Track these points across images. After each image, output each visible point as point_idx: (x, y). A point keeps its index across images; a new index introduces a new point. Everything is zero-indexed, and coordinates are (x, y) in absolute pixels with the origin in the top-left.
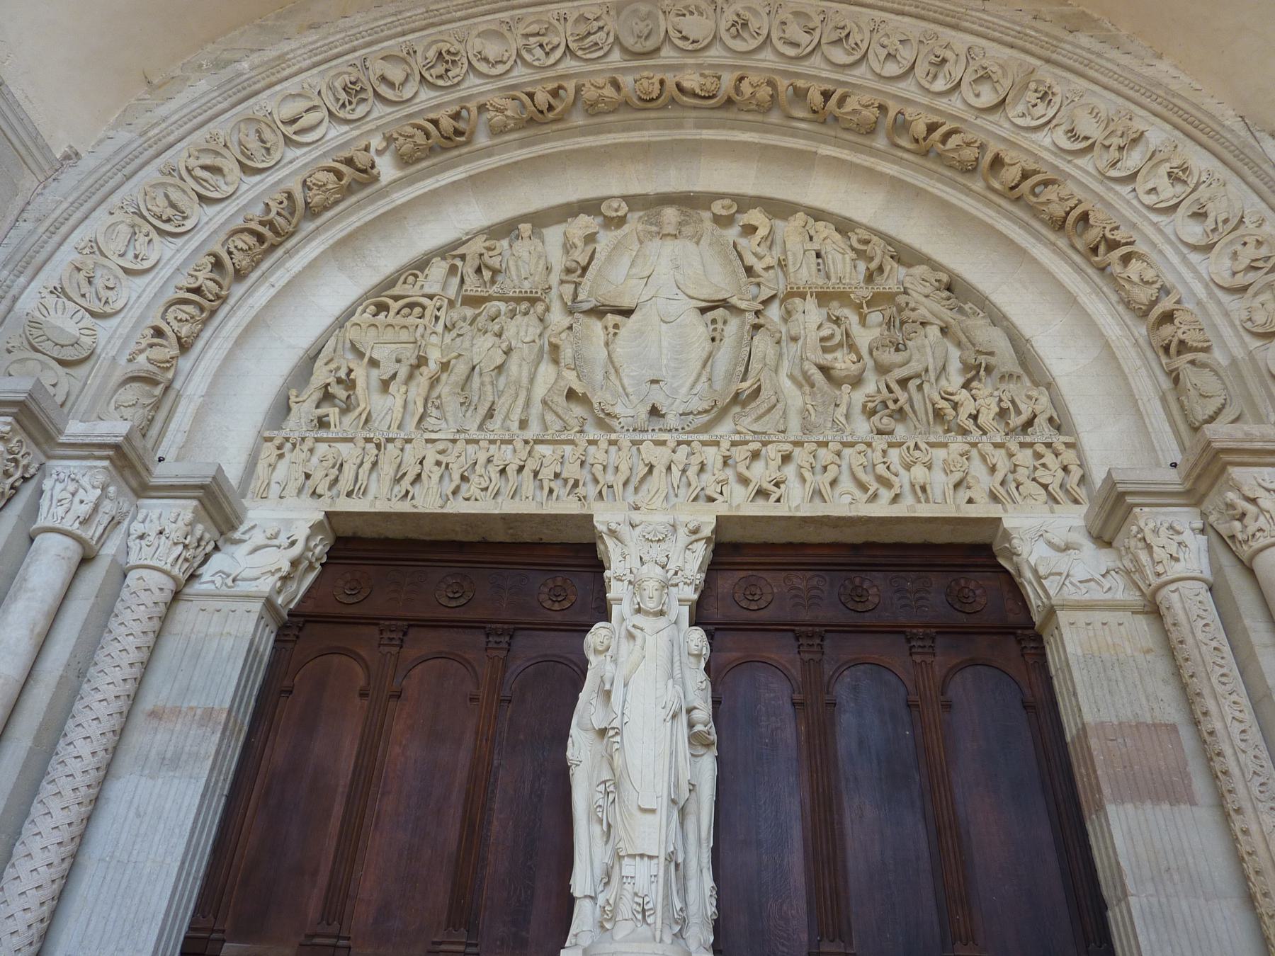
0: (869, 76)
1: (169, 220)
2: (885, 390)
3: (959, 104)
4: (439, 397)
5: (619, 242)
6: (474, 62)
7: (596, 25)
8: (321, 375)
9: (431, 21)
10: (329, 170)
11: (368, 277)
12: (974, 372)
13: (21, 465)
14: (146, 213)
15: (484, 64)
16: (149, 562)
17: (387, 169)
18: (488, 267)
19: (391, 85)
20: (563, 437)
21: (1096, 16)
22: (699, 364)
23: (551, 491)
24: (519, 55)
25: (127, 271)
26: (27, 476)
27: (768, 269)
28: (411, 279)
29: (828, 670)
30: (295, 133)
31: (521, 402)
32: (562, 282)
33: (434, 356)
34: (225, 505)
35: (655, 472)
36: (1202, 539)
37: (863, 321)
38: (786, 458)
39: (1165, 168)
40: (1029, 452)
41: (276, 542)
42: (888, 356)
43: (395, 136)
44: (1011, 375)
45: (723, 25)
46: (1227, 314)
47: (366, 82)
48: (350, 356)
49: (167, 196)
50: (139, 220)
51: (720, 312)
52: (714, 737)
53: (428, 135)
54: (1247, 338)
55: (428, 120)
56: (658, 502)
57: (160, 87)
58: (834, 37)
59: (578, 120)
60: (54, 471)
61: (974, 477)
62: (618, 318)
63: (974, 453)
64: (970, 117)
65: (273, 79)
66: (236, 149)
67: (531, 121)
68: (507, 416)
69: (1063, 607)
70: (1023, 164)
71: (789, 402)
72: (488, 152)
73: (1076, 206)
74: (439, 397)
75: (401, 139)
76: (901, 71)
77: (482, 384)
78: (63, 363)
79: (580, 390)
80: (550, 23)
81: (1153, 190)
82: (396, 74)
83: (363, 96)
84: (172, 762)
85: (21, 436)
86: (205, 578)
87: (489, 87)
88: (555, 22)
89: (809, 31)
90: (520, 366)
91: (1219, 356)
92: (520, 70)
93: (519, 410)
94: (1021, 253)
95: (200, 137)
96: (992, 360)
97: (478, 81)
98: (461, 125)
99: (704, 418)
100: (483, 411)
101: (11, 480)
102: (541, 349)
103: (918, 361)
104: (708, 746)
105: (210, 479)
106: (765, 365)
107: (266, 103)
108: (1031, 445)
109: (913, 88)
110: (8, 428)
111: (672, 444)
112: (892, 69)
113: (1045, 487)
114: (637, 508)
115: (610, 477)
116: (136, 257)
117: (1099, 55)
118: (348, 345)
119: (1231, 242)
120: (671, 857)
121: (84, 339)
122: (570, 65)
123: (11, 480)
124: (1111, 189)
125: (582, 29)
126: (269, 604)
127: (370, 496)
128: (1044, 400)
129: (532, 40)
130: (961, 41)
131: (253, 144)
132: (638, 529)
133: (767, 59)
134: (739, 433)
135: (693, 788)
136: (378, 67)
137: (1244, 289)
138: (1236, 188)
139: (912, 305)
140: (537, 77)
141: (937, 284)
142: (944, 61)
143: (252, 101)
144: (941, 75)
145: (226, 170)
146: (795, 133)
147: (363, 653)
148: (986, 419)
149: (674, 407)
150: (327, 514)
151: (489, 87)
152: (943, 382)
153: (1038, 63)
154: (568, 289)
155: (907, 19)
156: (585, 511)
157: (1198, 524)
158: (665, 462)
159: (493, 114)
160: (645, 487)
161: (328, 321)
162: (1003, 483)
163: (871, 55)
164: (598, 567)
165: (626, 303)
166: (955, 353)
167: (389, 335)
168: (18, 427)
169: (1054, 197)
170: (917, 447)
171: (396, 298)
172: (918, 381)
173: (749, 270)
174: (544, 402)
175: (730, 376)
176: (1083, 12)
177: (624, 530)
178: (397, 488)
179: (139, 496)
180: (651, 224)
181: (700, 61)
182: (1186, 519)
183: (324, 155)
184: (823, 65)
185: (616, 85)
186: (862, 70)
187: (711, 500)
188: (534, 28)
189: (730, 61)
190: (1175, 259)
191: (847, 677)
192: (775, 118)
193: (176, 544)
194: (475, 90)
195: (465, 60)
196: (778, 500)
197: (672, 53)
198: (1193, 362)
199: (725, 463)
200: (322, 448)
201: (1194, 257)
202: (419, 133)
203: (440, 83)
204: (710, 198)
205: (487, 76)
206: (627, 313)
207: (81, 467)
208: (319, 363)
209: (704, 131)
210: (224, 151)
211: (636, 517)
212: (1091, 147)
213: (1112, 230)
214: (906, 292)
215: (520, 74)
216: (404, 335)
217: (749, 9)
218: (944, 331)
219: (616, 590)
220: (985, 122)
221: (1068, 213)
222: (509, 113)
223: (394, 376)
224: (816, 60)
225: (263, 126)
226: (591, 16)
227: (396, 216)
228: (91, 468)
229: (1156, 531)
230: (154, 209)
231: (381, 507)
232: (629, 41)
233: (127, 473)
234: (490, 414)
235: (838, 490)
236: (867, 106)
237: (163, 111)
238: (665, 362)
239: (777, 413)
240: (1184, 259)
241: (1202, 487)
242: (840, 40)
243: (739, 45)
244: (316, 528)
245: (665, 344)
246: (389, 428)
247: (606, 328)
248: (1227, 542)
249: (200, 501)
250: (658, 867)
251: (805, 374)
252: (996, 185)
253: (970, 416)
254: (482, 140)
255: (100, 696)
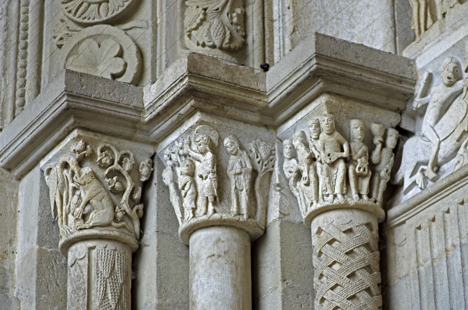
13: (125, 173)
16: (317, 206)
26: (144, 179)
34: (366, 76)
60: (165, 157)
85: (104, 141)
101: (126, 196)
105: (314, 61)
110: (81, 143)
123: (126, 196)
168: (91, 135)
179: (276, 127)
193: (333, 165)
207: (181, 135)
228: (189, 131)
233: (231, 111)
249: (329, 93)
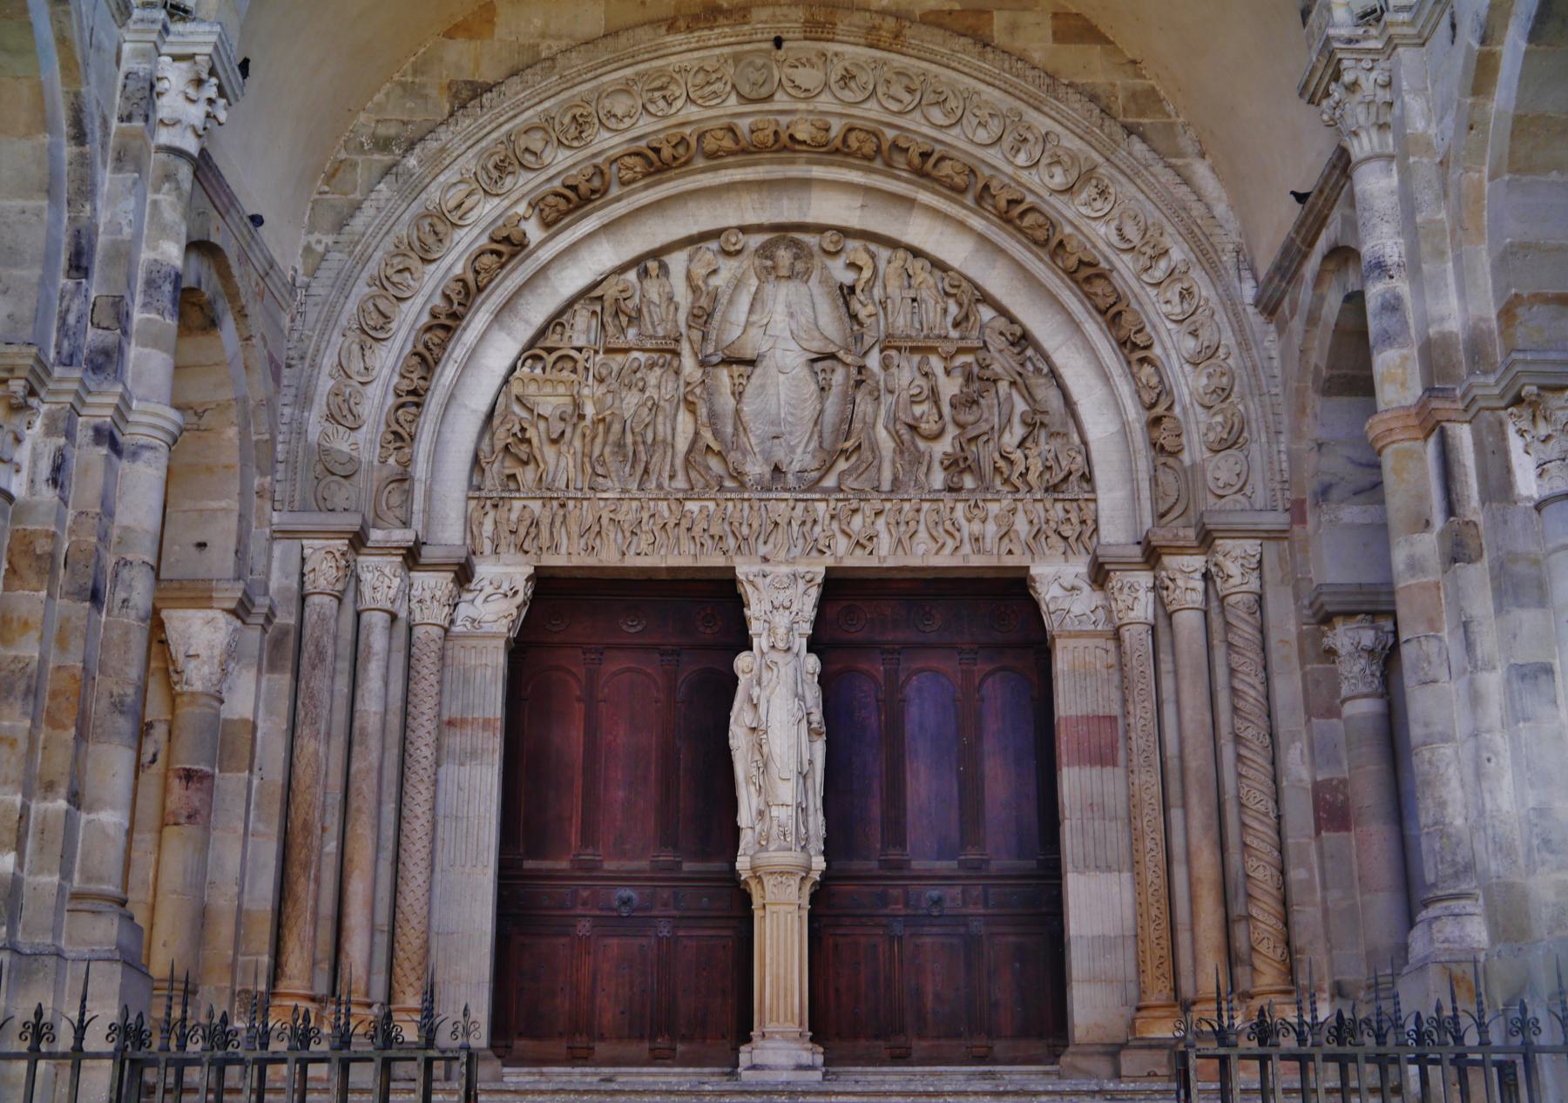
0: (963, 137)
1: (382, 328)
2: (958, 448)
3: (1036, 179)
4: (602, 454)
5: (739, 281)
6: (604, 120)
7: (714, 76)
8: (501, 436)
9: (564, 86)
10: (493, 252)
11: (525, 333)
12: (1033, 425)
14: (366, 328)
15: (613, 120)
17: (533, 231)
18: (623, 312)
19: (535, 154)
20: (707, 496)
21: (1162, 93)
22: (811, 425)
23: (702, 545)
24: (644, 107)
25: (362, 383)
27: (870, 316)
28: (559, 329)
29: (902, 677)
30: (460, 218)
31: (668, 459)
32: (690, 327)
33: (589, 410)
35: (780, 529)
36: (1151, 595)
37: (948, 372)
38: (878, 514)
39: (1178, 287)
40: (1059, 506)
41: (501, 591)
42: (967, 417)
43: (542, 206)
44: (1058, 434)
45: (833, 78)
46: (1197, 423)
47: (513, 157)
48: (517, 408)
49: (375, 305)
50: (364, 337)
51: (827, 364)
52: (824, 729)
53: (568, 200)
54: (1204, 448)
55: (568, 187)
56: (782, 555)
57: (333, 175)
58: (933, 98)
59: (700, 163)
61: (1016, 532)
62: (742, 369)
63: (1020, 505)
64: (1045, 194)
65: (437, 170)
66: (417, 244)
67: (659, 171)
68: (660, 474)
69: (1060, 636)
70: (1080, 254)
71: (884, 453)
72: (618, 199)
73: (1115, 303)
74: (602, 454)
75: (547, 209)
76: (989, 142)
77: (635, 443)
78: (346, 477)
79: (716, 446)
80: (672, 78)
81: (1167, 302)
82: (536, 141)
83: (510, 169)
84: (473, 755)
86: (459, 622)
87: (618, 139)
88: (677, 76)
89: (910, 91)
90: (665, 424)
91: (1186, 457)
92: (646, 119)
93: (668, 468)
94: (1076, 326)
95: (389, 244)
96: (1046, 420)
97: (607, 135)
98: (596, 183)
99: (815, 475)
100: (639, 470)
102: (678, 404)
103: (987, 420)
104: (820, 734)
106: (865, 423)
107: (433, 195)
108: (1064, 500)
109: (1000, 156)
111: (791, 503)
112: (982, 135)
113: (1065, 539)
114: (765, 560)
115: (745, 530)
116: (367, 369)
117: (1146, 168)
118: (514, 398)
119: (1208, 366)
120: (799, 805)
121: (354, 454)
122: (693, 112)
124: (1143, 288)
125: (700, 79)
126: (508, 641)
127: (563, 550)
128: (1079, 459)
129: (657, 94)
130: (1042, 123)
131: (431, 240)
132: (768, 579)
133: (872, 111)
134: (842, 491)
135: (811, 762)
136: (523, 142)
137: (1211, 407)
138: (1220, 317)
139: (988, 362)
140: (660, 126)
141: (1010, 338)
142: (1025, 140)
143: (423, 196)
144: (1022, 152)
145: (413, 269)
146: (898, 178)
147: (574, 670)
148: (1032, 477)
149: (792, 467)
150: (536, 568)
151: (618, 139)
152: (1006, 437)
153: (1100, 160)
154: (696, 335)
155: (997, 93)
156: (729, 564)
157: (1150, 585)
158: (786, 520)
159: (623, 172)
160: (772, 539)
161: (498, 381)
162: (1034, 537)
163: (965, 121)
164: (739, 603)
165: (749, 354)
166: (1021, 406)
167: (548, 389)
169: (1099, 292)
170: (976, 506)
171: (550, 350)
172: (985, 438)
173: (854, 317)
174: (687, 460)
175: (836, 430)
176: (1153, 89)
177: (759, 581)
178: (583, 541)
179: (410, 569)
180: (767, 258)
181: (811, 108)
182: (1144, 579)
183: (483, 231)
184: (923, 121)
185: (731, 129)
186: (956, 131)
187: (822, 552)
188: (657, 84)
189: (839, 109)
190: (1176, 365)
191: (914, 681)
192: (878, 164)
194: (605, 145)
195: (596, 121)
196: (871, 553)
197: (785, 98)
198: (1164, 464)
199: (832, 517)
200: (517, 505)
201: (1187, 368)
202: (562, 201)
203: (575, 144)
204: (820, 229)
205: (616, 130)
206: (752, 363)
208: (496, 421)
209: (815, 168)
210: (411, 254)
211: (767, 568)
212: (1134, 248)
213: (1136, 333)
214: (985, 346)
215: (645, 125)
216: (561, 389)
217: (857, 65)
218: (1013, 383)
219: (755, 627)
220: (1057, 201)
221: (1108, 309)
222: (638, 169)
223: (563, 433)
224: (917, 115)
225: (436, 220)
226: (709, 69)
227: (544, 270)
229: (1121, 589)
230: (372, 323)
231: (575, 561)
232: (746, 89)
234: (646, 471)
235: (916, 539)
236: (958, 174)
237: (358, 222)
238: (783, 415)
239: (873, 471)
240: (1181, 367)
241: (1152, 562)
242: (938, 103)
243: (847, 95)
244: (527, 580)
245: (782, 397)
246: (567, 487)
247: (732, 377)
248: (1161, 598)
250: (791, 811)
251: (897, 432)
252: (1060, 264)
253: (1021, 474)
254: (615, 191)
255: (426, 717)
